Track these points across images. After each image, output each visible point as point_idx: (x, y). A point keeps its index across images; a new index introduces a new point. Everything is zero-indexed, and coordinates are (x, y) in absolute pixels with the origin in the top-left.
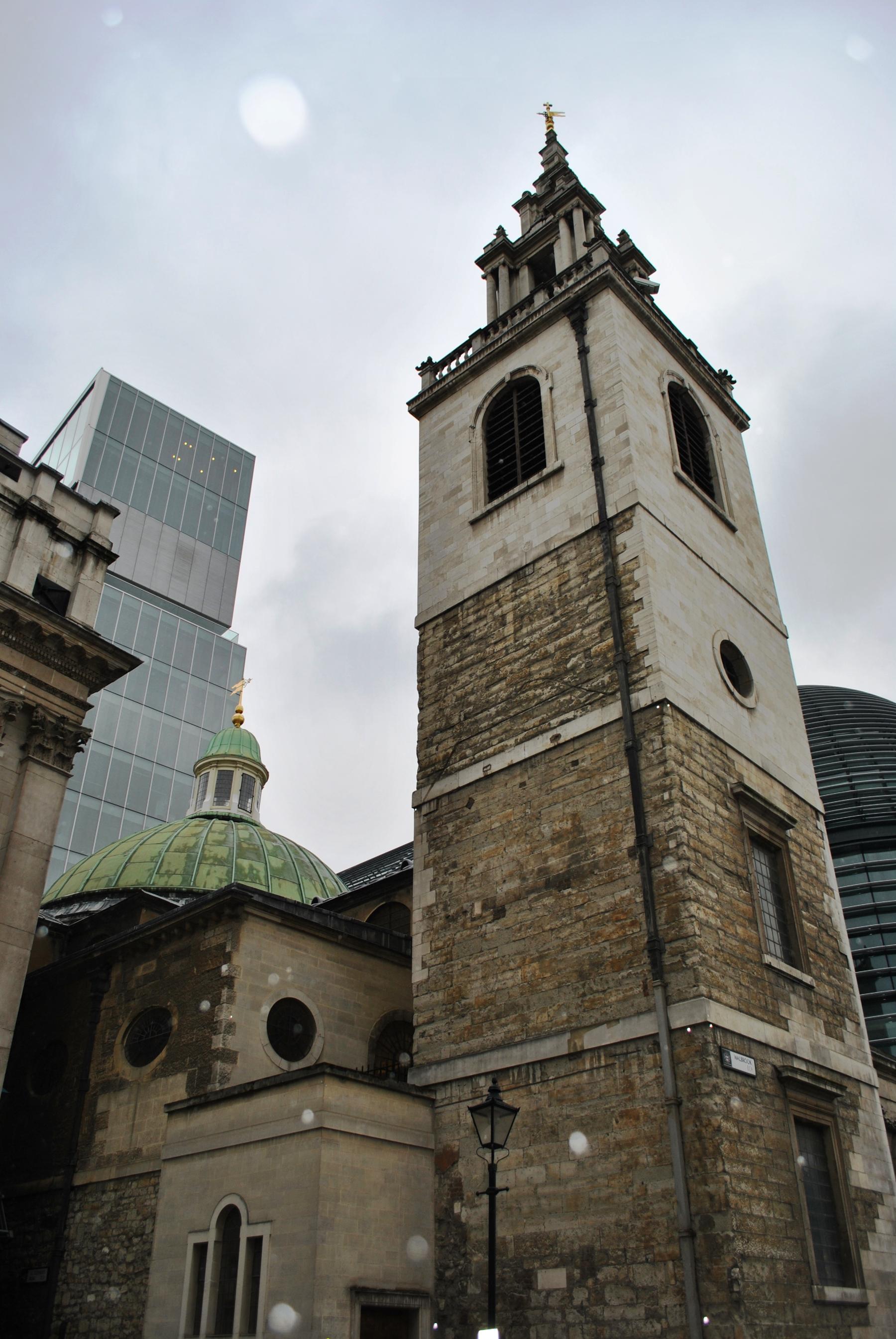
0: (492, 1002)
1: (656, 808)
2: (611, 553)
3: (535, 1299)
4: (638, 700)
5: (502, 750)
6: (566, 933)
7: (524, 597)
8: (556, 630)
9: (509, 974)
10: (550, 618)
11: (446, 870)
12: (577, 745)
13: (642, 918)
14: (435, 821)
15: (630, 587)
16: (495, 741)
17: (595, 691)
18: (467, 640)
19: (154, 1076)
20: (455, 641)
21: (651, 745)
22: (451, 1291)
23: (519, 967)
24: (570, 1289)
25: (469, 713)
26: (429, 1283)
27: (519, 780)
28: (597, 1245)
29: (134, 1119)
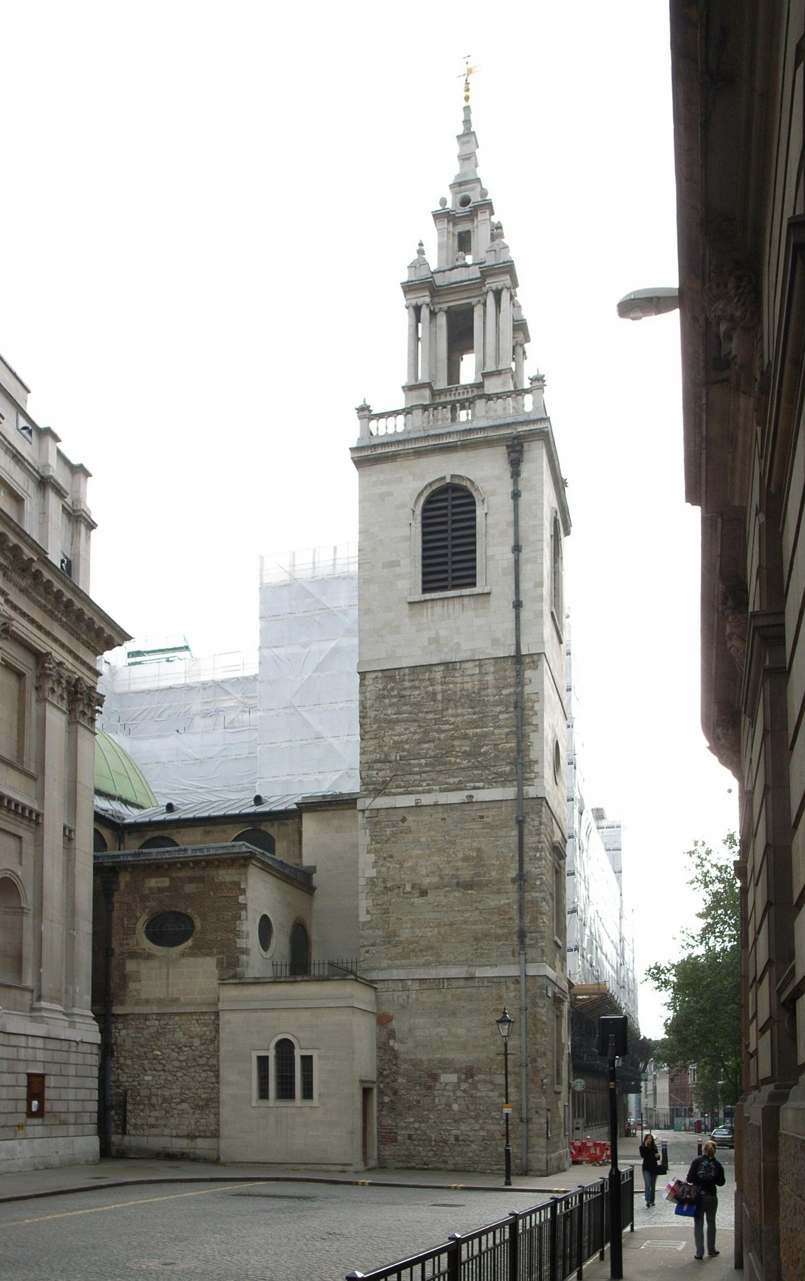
0: (417, 942)
1: (531, 859)
2: (520, 682)
3: (438, 1086)
4: (528, 792)
5: (429, 791)
6: (467, 915)
7: (451, 686)
8: (474, 721)
9: (430, 929)
10: (470, 710)
11: (385, 859)
12: (484, 806)
13: (516, 917)
14: (376, 824)
15: (531, 713)
16: (424, 784)
17: (500, 775)
18: (403, 700)
19: (183, 955)
20: (392, 696)
21: (531, 823)
22: (388, 1080)
23: (436, 927)
24: (459, 1083)
25: (404, 756)
26: (374, 1078)
27: (440, 815)
28: (475, 1066)
29: (168, 979)
